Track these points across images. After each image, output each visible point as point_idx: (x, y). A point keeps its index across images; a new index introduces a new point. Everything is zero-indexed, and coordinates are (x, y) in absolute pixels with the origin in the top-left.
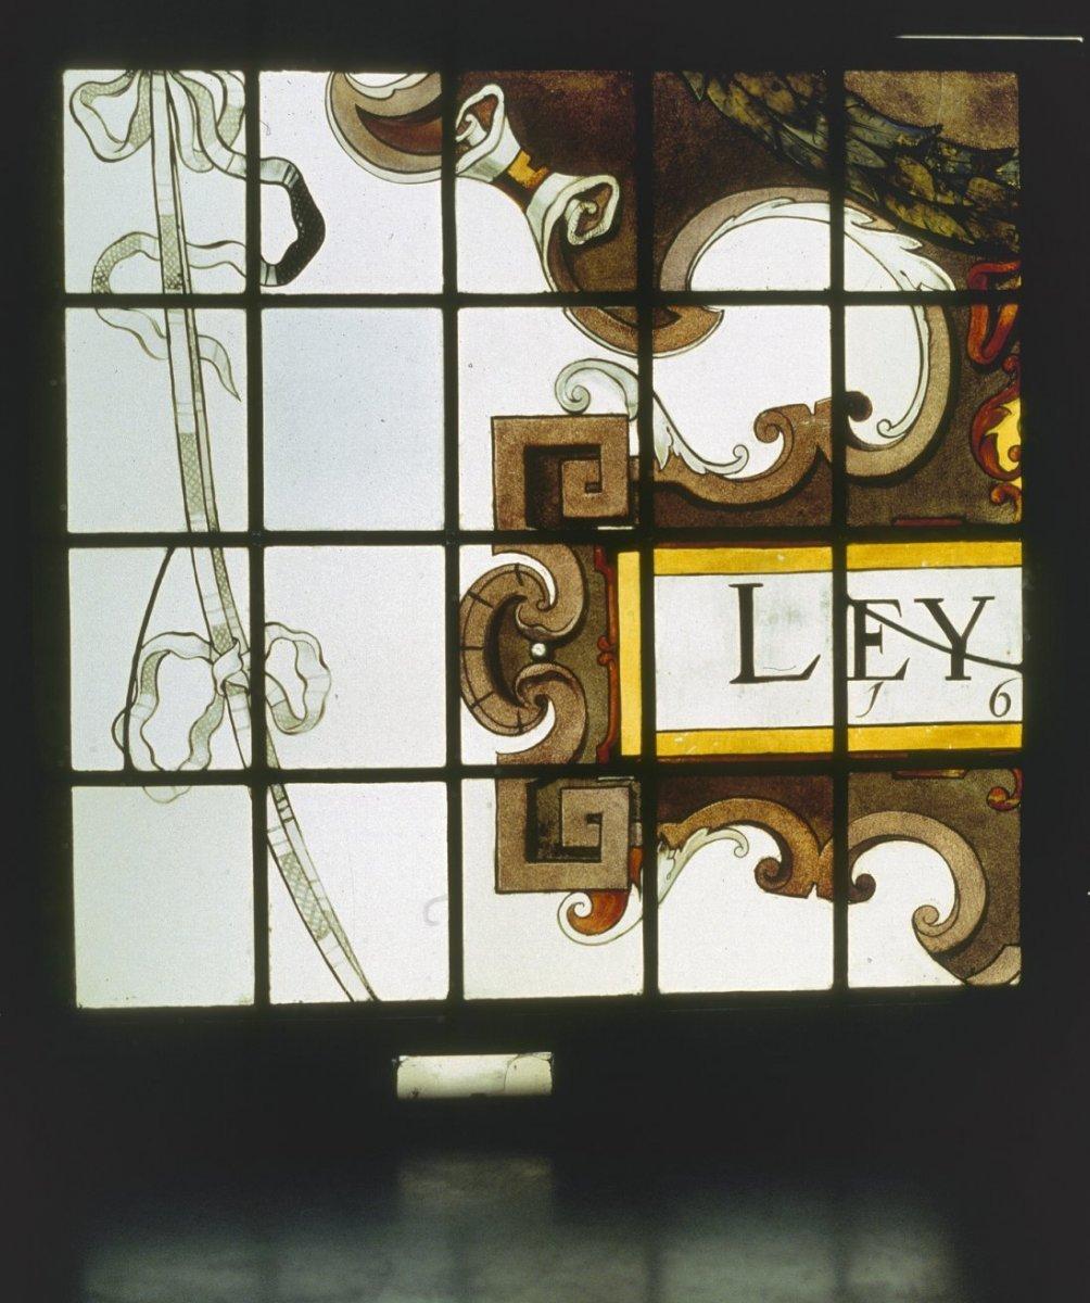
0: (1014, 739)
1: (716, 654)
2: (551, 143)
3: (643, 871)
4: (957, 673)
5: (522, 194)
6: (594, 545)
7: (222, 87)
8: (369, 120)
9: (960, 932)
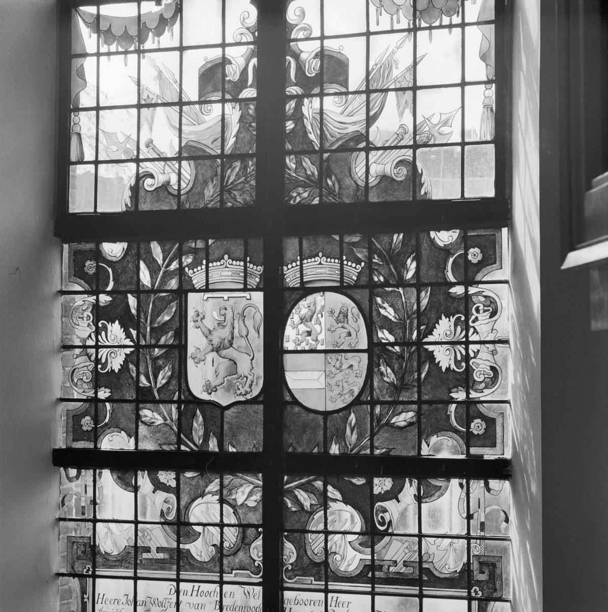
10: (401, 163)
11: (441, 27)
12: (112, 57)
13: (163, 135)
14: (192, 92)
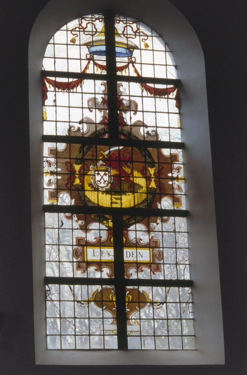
0: (113, 261)
1: (92, 254)
2: (79, 219)
3: (87, 269)
4: (109, 256)
5: (77, 222)
6: (83, 246)
7: (56, 214)
8: (66, 216)
9: (109, 275)
10: (152, 131)
11: (162, 98)
12: (59, 93)
13: (77, 115)
14: (86, 105)
